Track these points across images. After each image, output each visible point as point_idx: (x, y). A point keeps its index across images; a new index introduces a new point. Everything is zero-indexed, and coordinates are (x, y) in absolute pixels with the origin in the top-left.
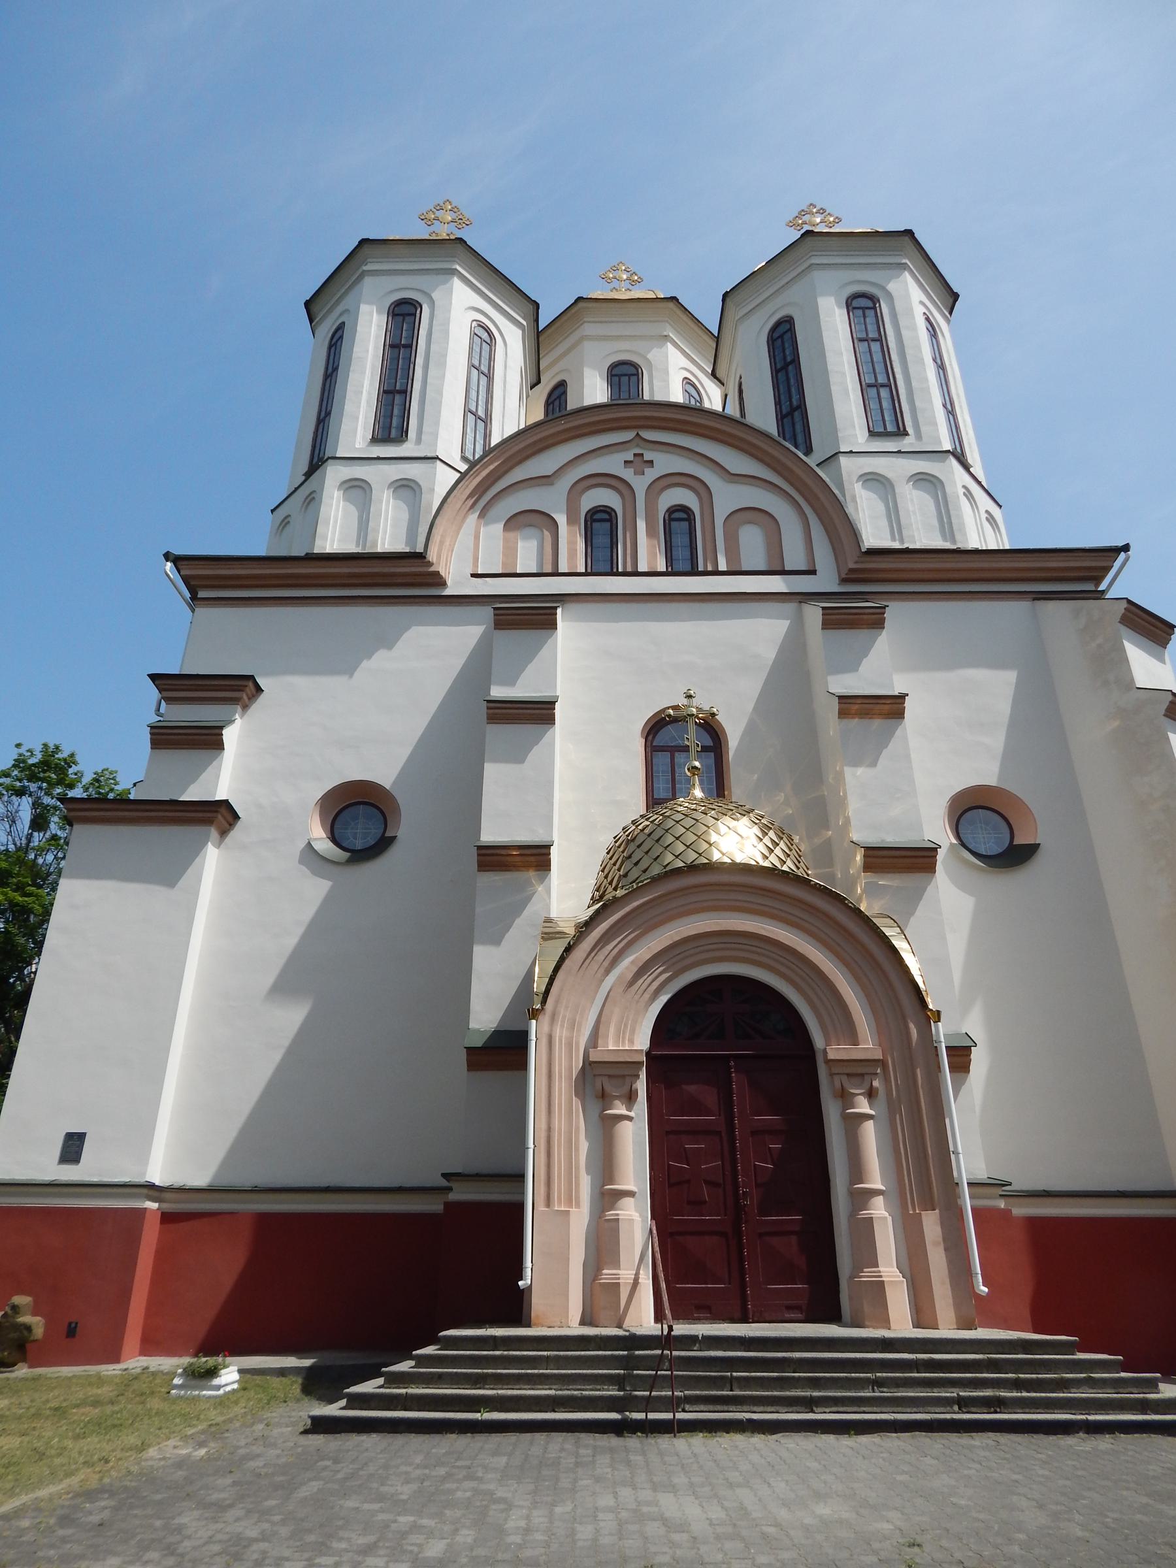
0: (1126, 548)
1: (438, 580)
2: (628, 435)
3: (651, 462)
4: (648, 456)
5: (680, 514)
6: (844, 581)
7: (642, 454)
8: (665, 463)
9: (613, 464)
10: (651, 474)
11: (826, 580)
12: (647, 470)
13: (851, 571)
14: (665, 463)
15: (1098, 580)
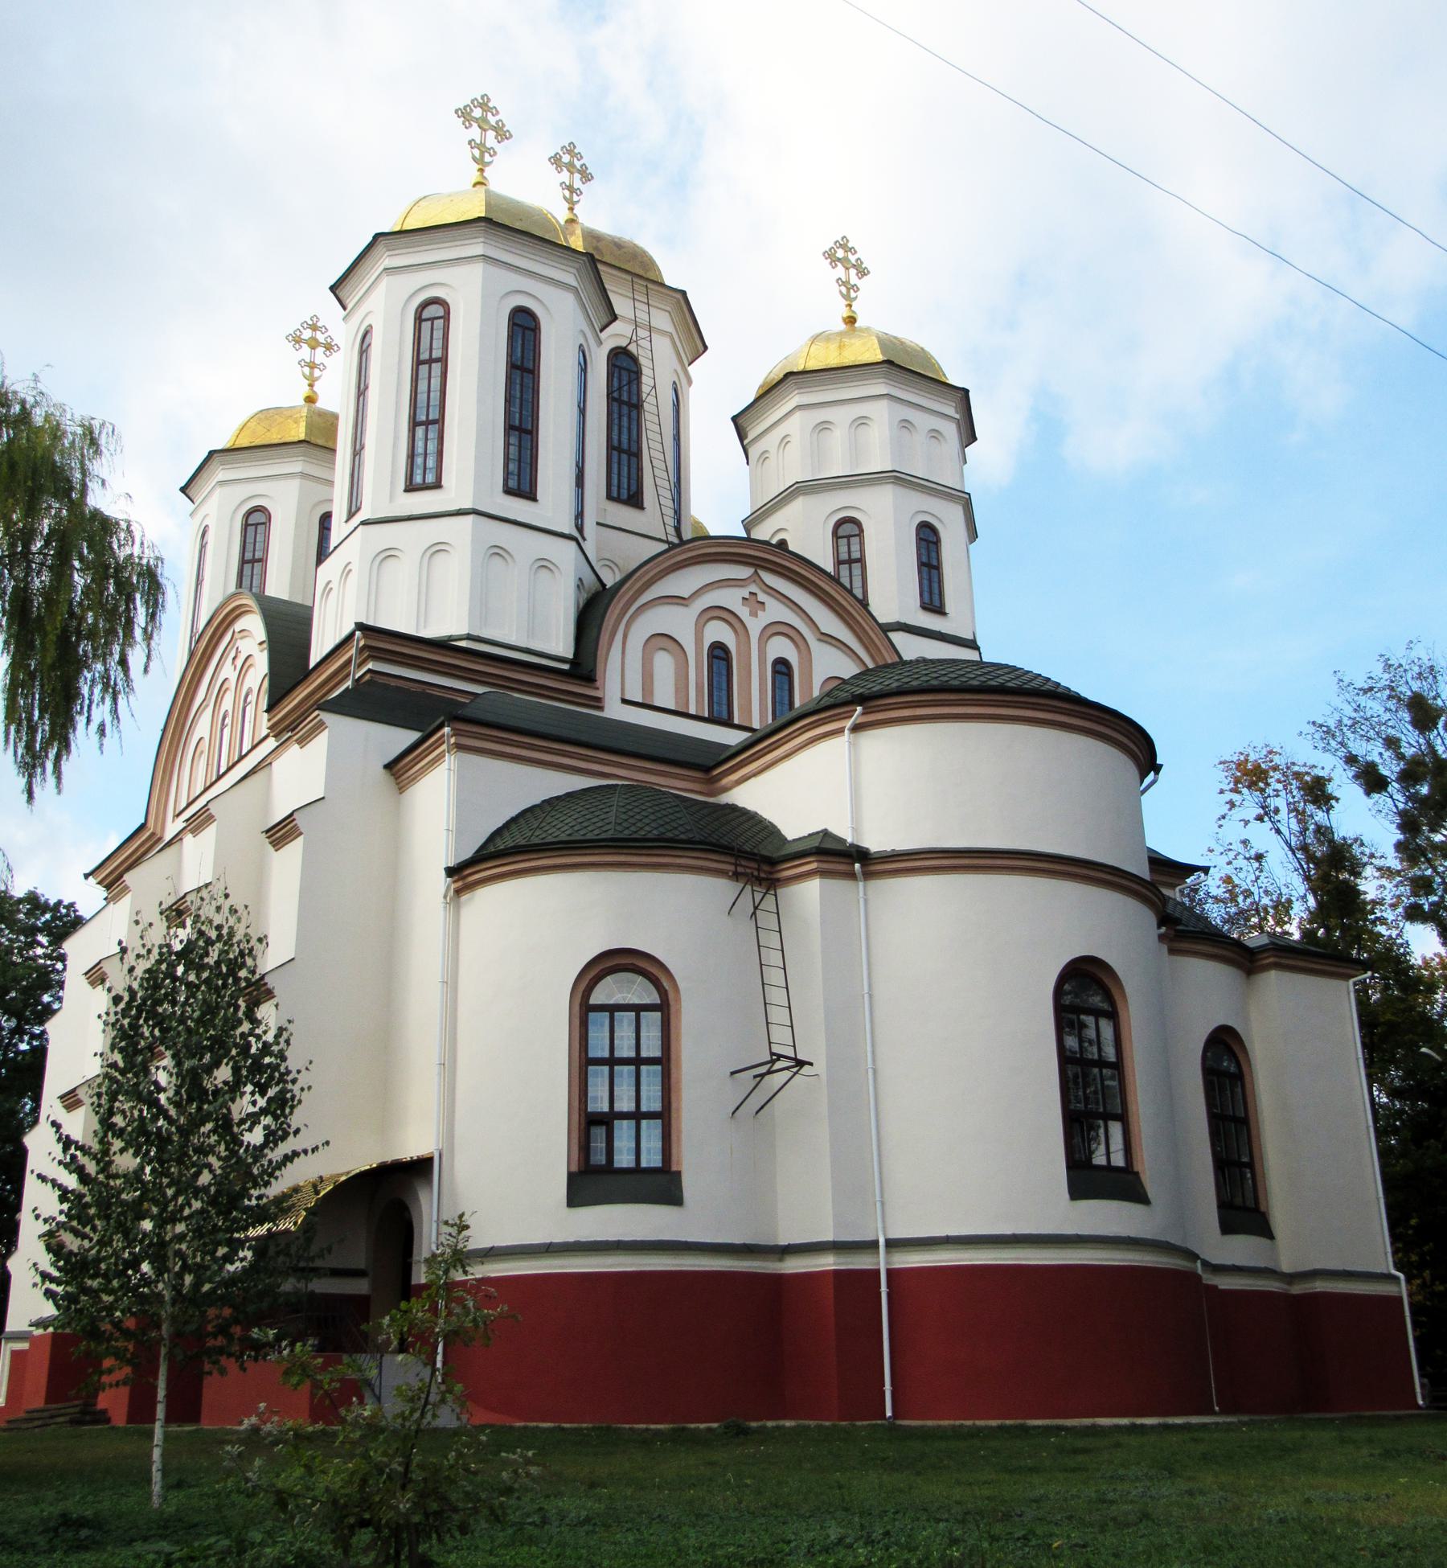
1: (597, 703)
2: (744, 572)
3: (763, 603)
4: (762, 597)
5: (782, 667)
7: (755, 594)
8: (776, 611)
9: (731, 599)
10: (765, 618)
12: (760, 613)
14: (776, 611)
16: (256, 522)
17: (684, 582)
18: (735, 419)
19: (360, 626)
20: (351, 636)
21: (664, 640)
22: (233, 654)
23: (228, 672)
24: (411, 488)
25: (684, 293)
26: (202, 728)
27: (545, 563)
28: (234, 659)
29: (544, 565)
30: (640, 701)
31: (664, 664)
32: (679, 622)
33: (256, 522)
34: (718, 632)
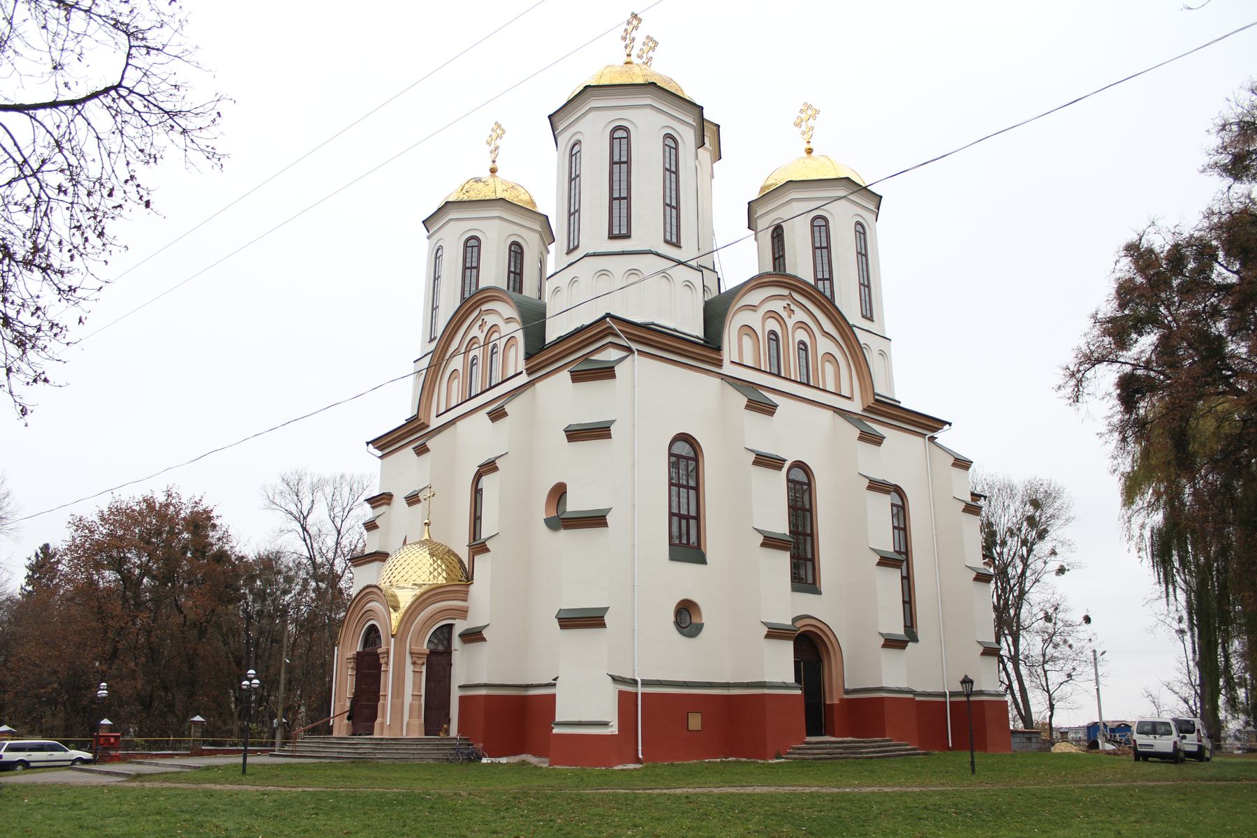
0: (950, 424)
1: (719, 363)
2: (785, 292)
3: (793, 311)
4: (793, 307)
6: (864, 410)
8: (800, 315)
9: (778, 306)
11: (856, 406)
12: (792, 315)
13: (869, 406)
15: (936, 430)
16: (472, 246)
17: (755, 297)
18: (749, 203)
19: (608, 315)
20: (604, 318)
21: (748, 329)
22: (480, 323)
23: (475, 331)
24: (612, 237)
25: (718, 126)
26: (457, 363)
27: (689, 284)
28: (480, 326)
29: (689, 285)
30: (738, 362)
31: (747, 342)
32: (754, 320)
33: (472, 246)
34: (772, 325)
